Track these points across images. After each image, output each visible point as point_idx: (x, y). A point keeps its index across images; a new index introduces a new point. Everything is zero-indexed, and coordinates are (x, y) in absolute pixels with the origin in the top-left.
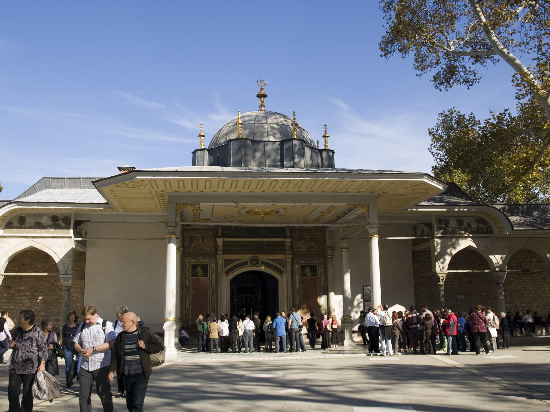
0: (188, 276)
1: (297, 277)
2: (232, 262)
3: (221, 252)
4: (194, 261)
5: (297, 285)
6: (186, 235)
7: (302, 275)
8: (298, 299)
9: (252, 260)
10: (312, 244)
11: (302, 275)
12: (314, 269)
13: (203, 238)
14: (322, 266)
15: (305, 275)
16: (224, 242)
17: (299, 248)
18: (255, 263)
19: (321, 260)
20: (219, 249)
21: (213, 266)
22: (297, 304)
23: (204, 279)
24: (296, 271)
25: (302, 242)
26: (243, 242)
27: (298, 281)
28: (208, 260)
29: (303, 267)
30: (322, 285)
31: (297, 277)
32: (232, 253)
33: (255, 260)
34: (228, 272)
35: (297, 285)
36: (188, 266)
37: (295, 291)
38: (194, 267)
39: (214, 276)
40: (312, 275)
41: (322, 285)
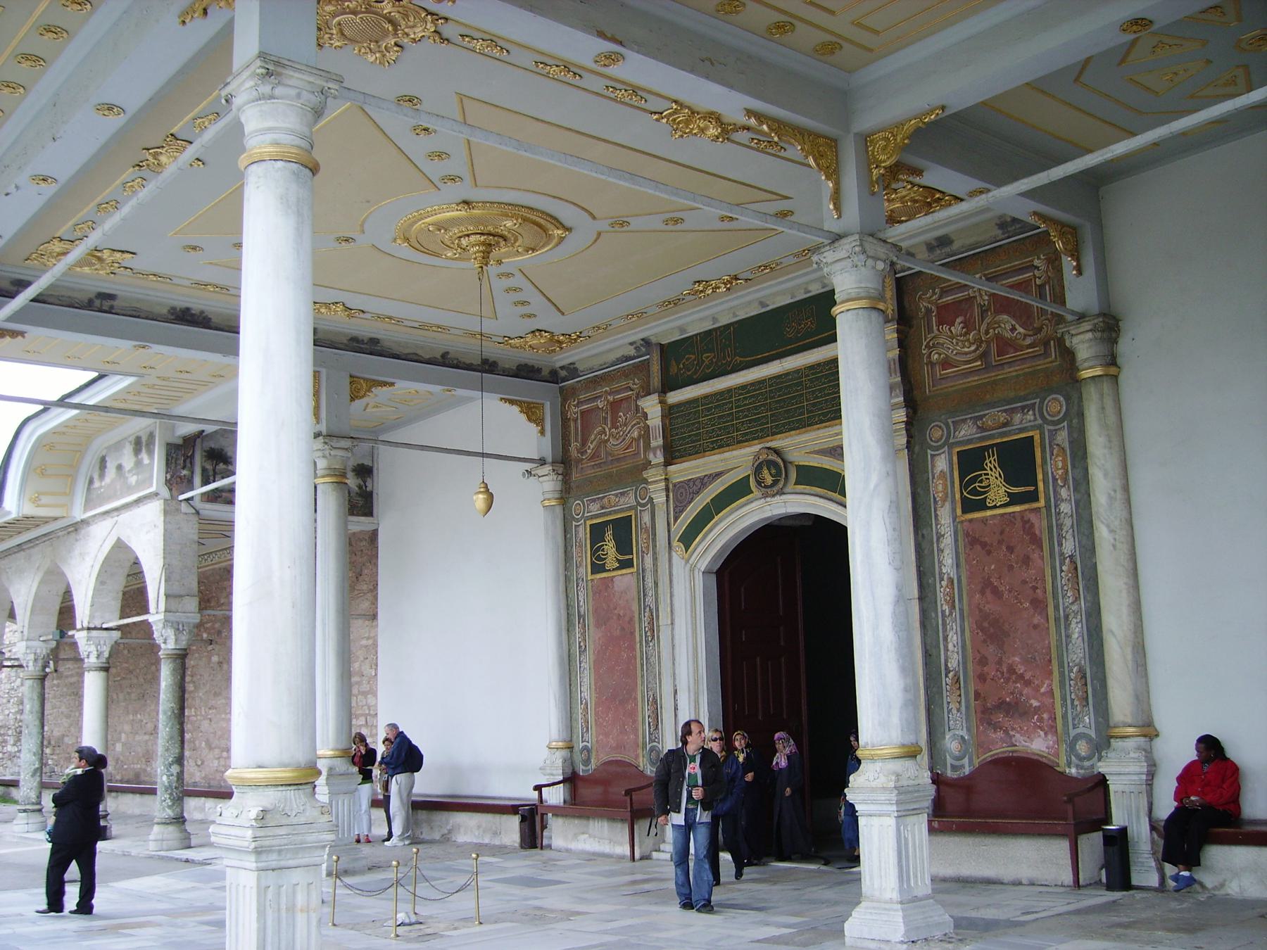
0: (582, 570)
1: (945, 519)
2: (698, 493)
3: (658, 458)
4: (595, 508)
5: (947, 563)
6: (574, 411)
7: (968, 506)
8: (953, 638)
9: (758, 470)
10: (1006, 322)
11: (968, 506)
12: (1019, 462)
13: (615, 406)
14: (1063, 437)
15: (982, 506)
16: (669, 412)
17: (946, 363)
18: (769, 480)
19: (1056, 405)
20: (654, 444)
21: (646, 518)
22: (953, 664)
23: (624, 580)
24: (937, 488)
25: (957, 328)
26: (729, 391)
27: (948, 541)
28: (630, 500)
29: (970, 462)
30: (1069, 546)
31: (945, 519)
32: (697, 451)
33: (770, 464)
34: (688, 538)
35: (947, 563)
36: (581, 534)
37: (940, 596)
38: (597, 533)
39: (648, 560)
40: (1014, 499)
41: (1069, 546)
